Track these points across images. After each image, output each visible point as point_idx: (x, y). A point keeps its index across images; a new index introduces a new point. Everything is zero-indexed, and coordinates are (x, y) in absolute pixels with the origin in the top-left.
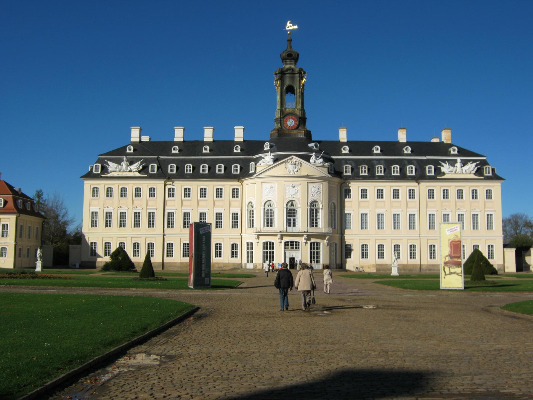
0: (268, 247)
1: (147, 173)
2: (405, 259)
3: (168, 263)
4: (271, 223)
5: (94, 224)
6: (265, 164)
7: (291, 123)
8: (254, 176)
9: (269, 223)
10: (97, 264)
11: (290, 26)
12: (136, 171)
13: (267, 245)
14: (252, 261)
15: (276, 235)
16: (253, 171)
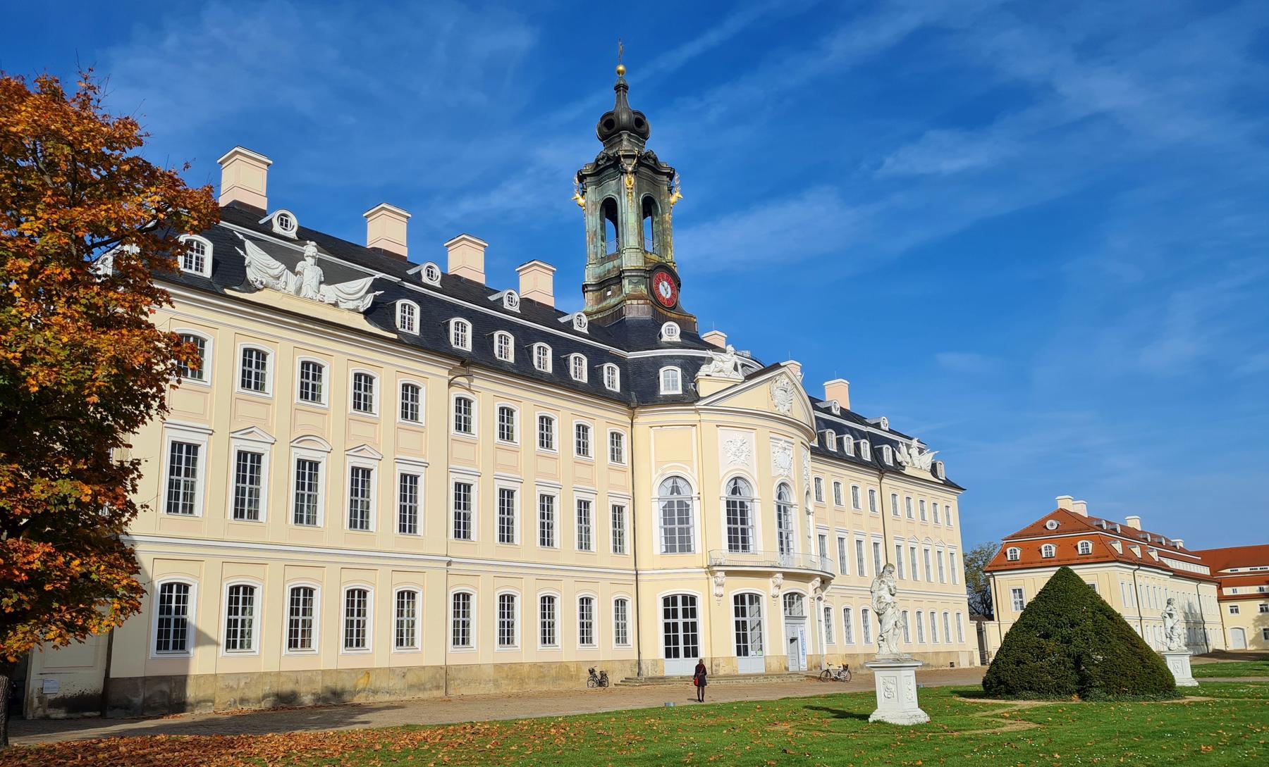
0: (681, 611)
1: (389, 325)
2: (432, 645)
3: (459, 668)
4: (744, 540)
5: (180, 499)
6: (721, 374)
7: (665, 290)
8: (700, 404)
9: (738, 538)
10: (191, 693)
11: (621, 68)
12: (356, 310)
13: (675, 603)
14: (692, 652)
15: (769, 575)
16: (680, 392)
